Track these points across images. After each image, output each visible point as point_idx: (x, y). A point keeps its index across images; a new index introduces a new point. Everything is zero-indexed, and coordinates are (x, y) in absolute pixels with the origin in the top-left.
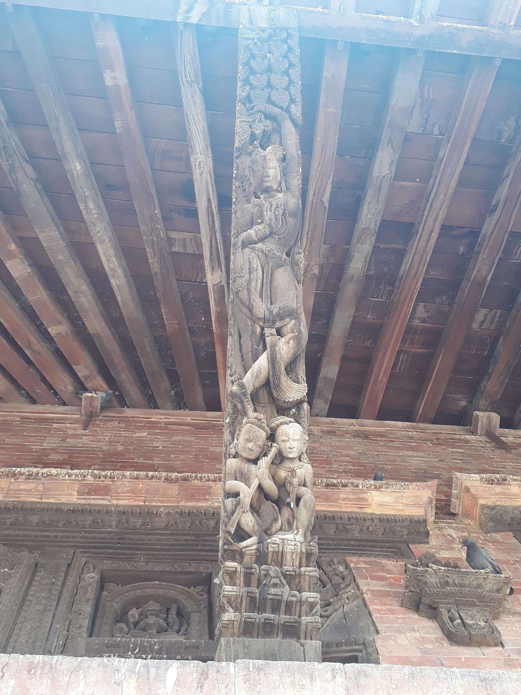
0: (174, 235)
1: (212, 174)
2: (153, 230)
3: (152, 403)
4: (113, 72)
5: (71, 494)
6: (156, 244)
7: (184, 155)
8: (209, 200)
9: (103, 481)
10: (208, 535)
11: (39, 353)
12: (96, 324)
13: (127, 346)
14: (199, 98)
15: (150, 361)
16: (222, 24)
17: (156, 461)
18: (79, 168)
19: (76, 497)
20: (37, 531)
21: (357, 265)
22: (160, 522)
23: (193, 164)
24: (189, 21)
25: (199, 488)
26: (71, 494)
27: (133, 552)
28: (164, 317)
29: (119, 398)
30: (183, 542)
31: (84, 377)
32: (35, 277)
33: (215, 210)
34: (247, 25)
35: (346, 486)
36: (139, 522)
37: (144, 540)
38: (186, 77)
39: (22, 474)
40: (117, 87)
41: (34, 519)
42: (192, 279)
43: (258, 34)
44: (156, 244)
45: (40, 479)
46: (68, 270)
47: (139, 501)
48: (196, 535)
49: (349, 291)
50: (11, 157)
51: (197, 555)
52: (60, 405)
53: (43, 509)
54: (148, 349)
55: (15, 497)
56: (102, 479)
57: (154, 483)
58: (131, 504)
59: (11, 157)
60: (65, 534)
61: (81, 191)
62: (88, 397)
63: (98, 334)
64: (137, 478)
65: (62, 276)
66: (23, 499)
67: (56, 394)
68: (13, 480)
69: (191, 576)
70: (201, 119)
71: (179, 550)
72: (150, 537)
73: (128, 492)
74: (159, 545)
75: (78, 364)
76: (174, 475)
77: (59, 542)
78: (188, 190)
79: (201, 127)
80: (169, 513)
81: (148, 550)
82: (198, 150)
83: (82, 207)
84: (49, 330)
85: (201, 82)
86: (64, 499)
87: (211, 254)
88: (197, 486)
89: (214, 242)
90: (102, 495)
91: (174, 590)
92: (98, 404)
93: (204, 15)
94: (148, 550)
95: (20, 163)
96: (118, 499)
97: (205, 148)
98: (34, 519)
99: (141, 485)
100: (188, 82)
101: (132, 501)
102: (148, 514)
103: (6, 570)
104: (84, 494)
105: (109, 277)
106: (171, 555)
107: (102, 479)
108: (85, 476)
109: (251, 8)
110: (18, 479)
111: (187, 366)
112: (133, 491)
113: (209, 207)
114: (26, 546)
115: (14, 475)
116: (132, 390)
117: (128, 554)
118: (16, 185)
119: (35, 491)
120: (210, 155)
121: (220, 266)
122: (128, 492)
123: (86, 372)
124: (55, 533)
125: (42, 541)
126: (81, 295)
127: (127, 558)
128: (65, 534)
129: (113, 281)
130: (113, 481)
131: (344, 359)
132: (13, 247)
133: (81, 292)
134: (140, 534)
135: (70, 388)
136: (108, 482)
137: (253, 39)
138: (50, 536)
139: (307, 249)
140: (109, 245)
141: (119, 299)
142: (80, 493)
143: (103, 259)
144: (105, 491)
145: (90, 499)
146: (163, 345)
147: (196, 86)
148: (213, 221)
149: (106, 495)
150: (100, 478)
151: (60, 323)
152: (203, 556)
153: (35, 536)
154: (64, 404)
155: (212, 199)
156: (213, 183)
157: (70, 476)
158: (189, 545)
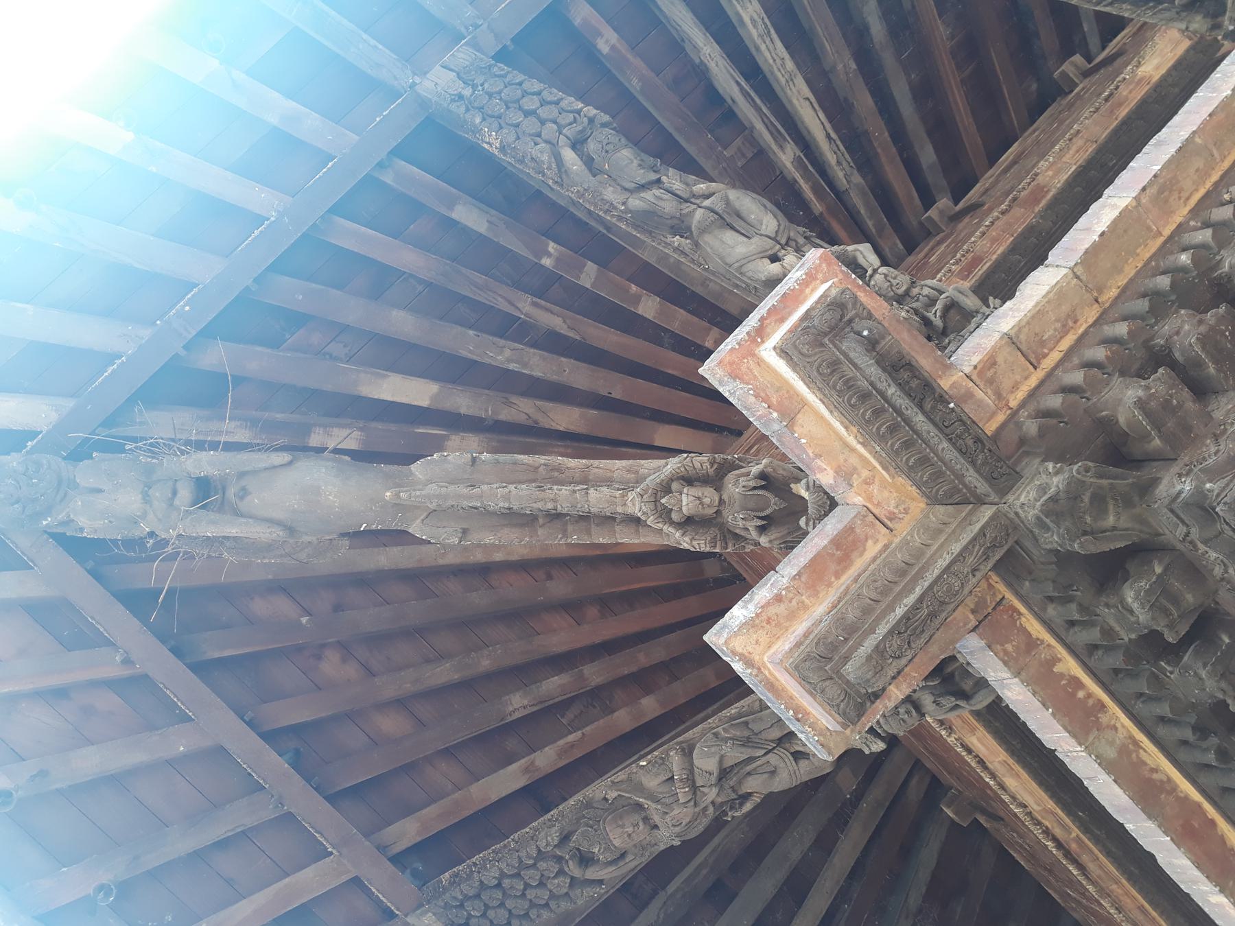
8: (738, 83)
21: (878, 30)
33: (747, 88)
35: (1117, 88)
49: (888, 59)
73: (992, 244)
78: (713, 97)
82: (701, 45)
87: (771, 134)
104: (968, 276)
121: (785, 139)
122: (992, 244)
131: (930, 133)
132: (634, 288)
142: (965, 278)
144: (977, 261)
148: (753, 100)
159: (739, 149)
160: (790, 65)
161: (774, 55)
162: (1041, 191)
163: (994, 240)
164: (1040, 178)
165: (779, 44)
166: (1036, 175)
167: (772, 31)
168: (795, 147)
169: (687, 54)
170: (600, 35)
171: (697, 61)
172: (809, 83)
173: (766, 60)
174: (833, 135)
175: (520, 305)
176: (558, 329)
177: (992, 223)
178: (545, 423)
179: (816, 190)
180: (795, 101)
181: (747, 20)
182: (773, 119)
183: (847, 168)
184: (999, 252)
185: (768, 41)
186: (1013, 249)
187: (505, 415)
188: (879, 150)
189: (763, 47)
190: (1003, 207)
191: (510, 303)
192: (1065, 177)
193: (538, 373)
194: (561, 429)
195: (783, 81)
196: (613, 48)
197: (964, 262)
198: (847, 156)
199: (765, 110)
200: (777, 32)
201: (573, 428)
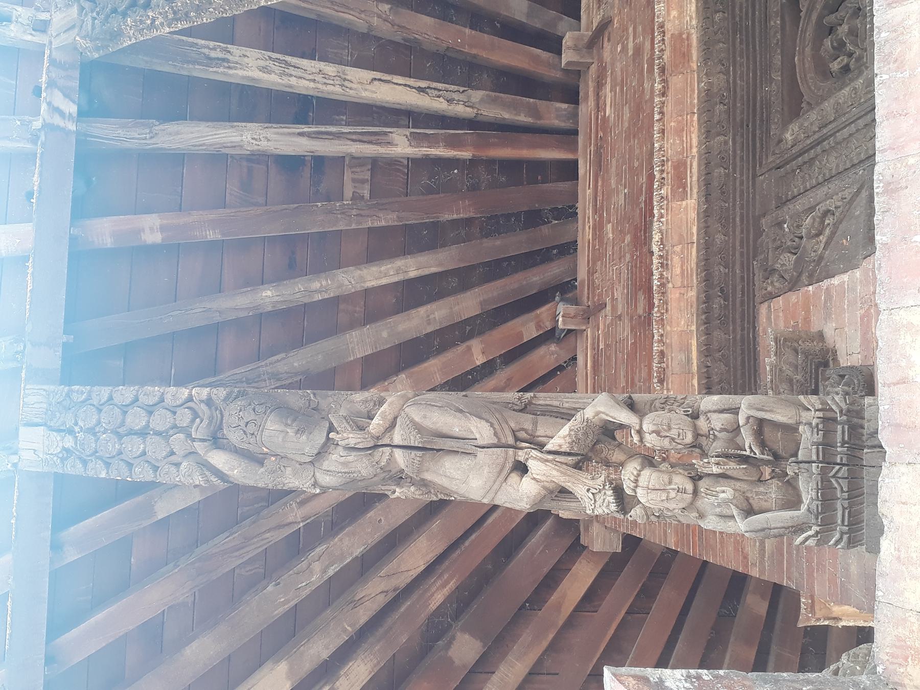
0: (348, 192)
1: (266, 125)
2: (343, 213)
3: (569, 248)
4: (143, 230)
5: (686, 208)
6: (361, 212)
7: (245, 163)
8: (301, 134)
9: (668, 173)
10: (734, 17)
11: (509, 380)
12: (468, 304)
13: (495, 269)
14: (172, 127)
15: (514, 243)
16: (77, 74)
17: (643, 179)
18: (269, 293)
19: (689, 201)
20: (734, 232)
22: (719, 81)
23: (256, 148)
24: (75, 115)
25: (674, 50)
26: (686, 208)
27: (758, 104)
28: (455, 216)
29: (565, 288)
30: (744, 46)
31: (538, 330)
32: (400, 9)
33: (313, 129)
34: (76, 30)
36: (719, 108)
37: (742, 96)
38: (146, 139)
39: (662, 275)
40: (163, 229)
41: (719, 238)
42: (403, 173)
43: (86, 14)
44: (361, 212)
45: (667, 252)
46: (401, 328)
47: (692, 121)
48: (735, 33)
50: (259, 376)
51: (760, 22)
52: (575, 365)
53: (706, 233)
54: (498, 243)
55: (692, 276)
56: (664, 175)
57: (668, 109)
58: (696, 131)
59: (259, 376)
60: (738, 196)
61: (298, 295)
62: (563, 321)
63: (481, 303)
64: (663, 132)
65: (409, 337)
66: (694, 265)
67: (560, 368)
68: (670, 285)
69: (787, 18)
70: (197, 129)
71: (754, 47)
72: (738, 90)
73: (681, 138)
74: (748, 75)
75: (520, 335)
76: (658, 86)
77: (748, 201)
78: (290, 164)
79: (208, 129)
80: (706, 74)
81: (755, 85)
82: (238, 139)
83: (318, 297)
84: (478, 363)
85: (151, 121)
86: (693, 215)
87: (370, 142)
88: (671, 52)
89: (354, 137)
90: (686, 168)
91: (805, 33)
92: (572, 309)
93: (66, 96)
94: (755, 85)
95: (266, 365)
96: (691, 148)
97: (234, 130)
98: (719, 238)
99: (673, 124)
100: (151, 138)
101: (692, 129)
102: (708, 98)
103: (785, 226)
104: (685, 192)
105: (406, 278)
106: (761, 55)
107: (664, 175)
108: (662, 197)
109: (54, 34)
110: (667, 278)
111: (519, 198)
112: (679, 132)
113: (309, 135)
114: (755, 241)
115: (663, 285)
116: (553, 271)
117: (762, 109)
118: (296, 374)
119: (682, 253)
120: (244, 124)
121: (385, 134)
122: (681, 138)
123: (532, 326)
124: (738, 209)
125: (748, 221)
126: (432, 317)
127: (766, 108)
128: (738, 196)
129: (413, 274)
130: (668, 160)
133: (428, 316)
134: (735, 105)
135: (553, 347)
136: (669, 167)
137: (94, 19)
138: (742, 214)
139: (357, 15)
140: (365, 271)
141: (434, 270)
143: (384, 281)
144: (680, 168)
145: (691, 181)
146: (494, 225)
147: (157, 128)
149: (685, 164)
150: (663, 178)
151: (469, 348)
152: (760, 14)
153: (742, 232)
154: (574, 359)
155: (298, 131)
156: (279, 125)
157: (662, 216)
158: (747, 36)
159: (354, 180)
160: (331, 69)
161: (310, 76)
162: (680, 39)
163: (679, 132)
164: (668, 26)
165: (305, 63)
166: (662, 26)
167: (289, 59)
168: (400, 131)
169: (232, 156)
170: (140, 231)
171: (248, 153)
172: (359, 64)
173: (307, 88)
174: (423, 84)
175: (291, 519)
176: (342, 499)
177: (661, 113)
178: (403, 581)
179: (452, 143)
180: (364, 94)
181: (257, 74)
182: (359, 129)
183: (462, 97)
184: (695, 142)
185: (291, 71)
186: (708, 133)
187: (363, 616)
188: (474, 51)
189: (293, 81)
190: (658, 86)
191: (280, 527)
192: (693, 8)
193: (358, 551)
194: (422, 568)
195: (338, 89)
196: (163, 229)
197: (669, 177)
198: (452, 87)
199: (346, 130)
200: (292, 55)
201: (431, 557)
